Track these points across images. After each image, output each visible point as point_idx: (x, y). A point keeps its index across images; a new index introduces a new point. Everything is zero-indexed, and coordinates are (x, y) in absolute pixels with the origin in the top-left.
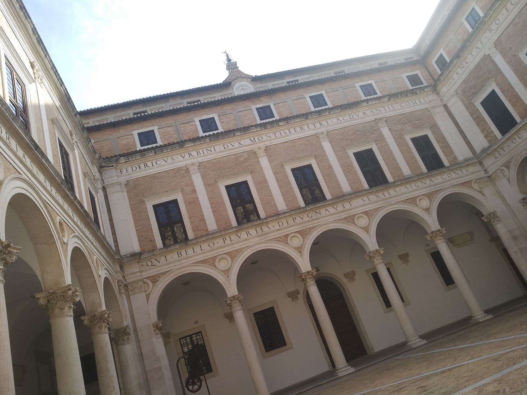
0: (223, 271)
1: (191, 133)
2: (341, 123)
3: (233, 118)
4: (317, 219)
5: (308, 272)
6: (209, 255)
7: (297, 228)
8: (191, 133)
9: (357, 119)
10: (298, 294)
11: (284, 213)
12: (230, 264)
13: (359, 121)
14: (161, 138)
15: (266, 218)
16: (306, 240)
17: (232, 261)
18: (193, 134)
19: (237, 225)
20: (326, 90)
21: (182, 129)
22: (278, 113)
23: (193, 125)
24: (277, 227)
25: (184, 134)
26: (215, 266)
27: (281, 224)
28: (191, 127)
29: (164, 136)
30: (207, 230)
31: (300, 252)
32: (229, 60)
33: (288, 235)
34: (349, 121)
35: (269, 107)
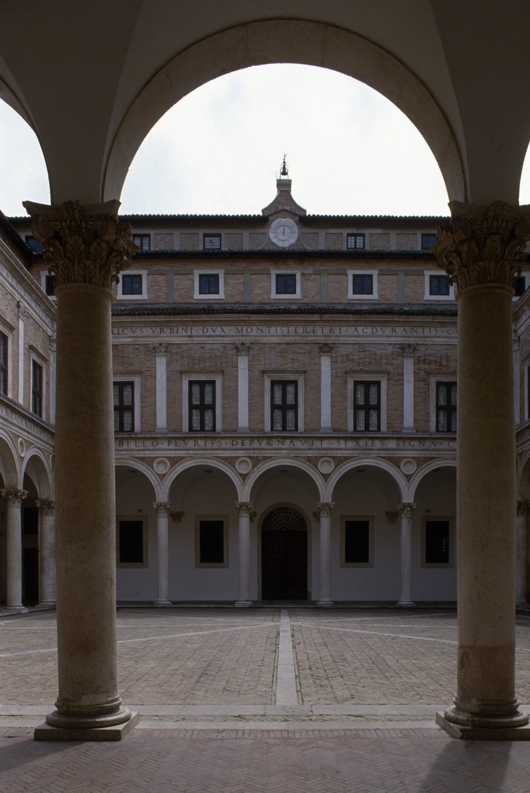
0: (159, 475)
1: (185, 290)
2: (357, 336)
3: (242, 281)
4: (277, 449)
5: (243, 503)
6: (147, 454)
7: (251, 453)
8: (185, 290)
9: (379, 336)
10: (255, 516)
11: (242, 433)
12: (167, 469)
13: (382, 339)
14: (148, 289)
15: (219, 433)
16: (255, 469)
17: (171, 467)
18: (186, 292)
19: (187, 430)
20: (380, 271)
21: (176, 281)
22: (303, 289)
23: (189, 280)
24: (229, 446)
25: (176, 289)
26: (152, 467)
27: (235, 443)
28: (187, 282)
29: (151, 286)
30: (156, 426)
31: (244, 479)
32: (284, 173)
33: (239, 457)
34: (368, 336)
35: (294, 276)
